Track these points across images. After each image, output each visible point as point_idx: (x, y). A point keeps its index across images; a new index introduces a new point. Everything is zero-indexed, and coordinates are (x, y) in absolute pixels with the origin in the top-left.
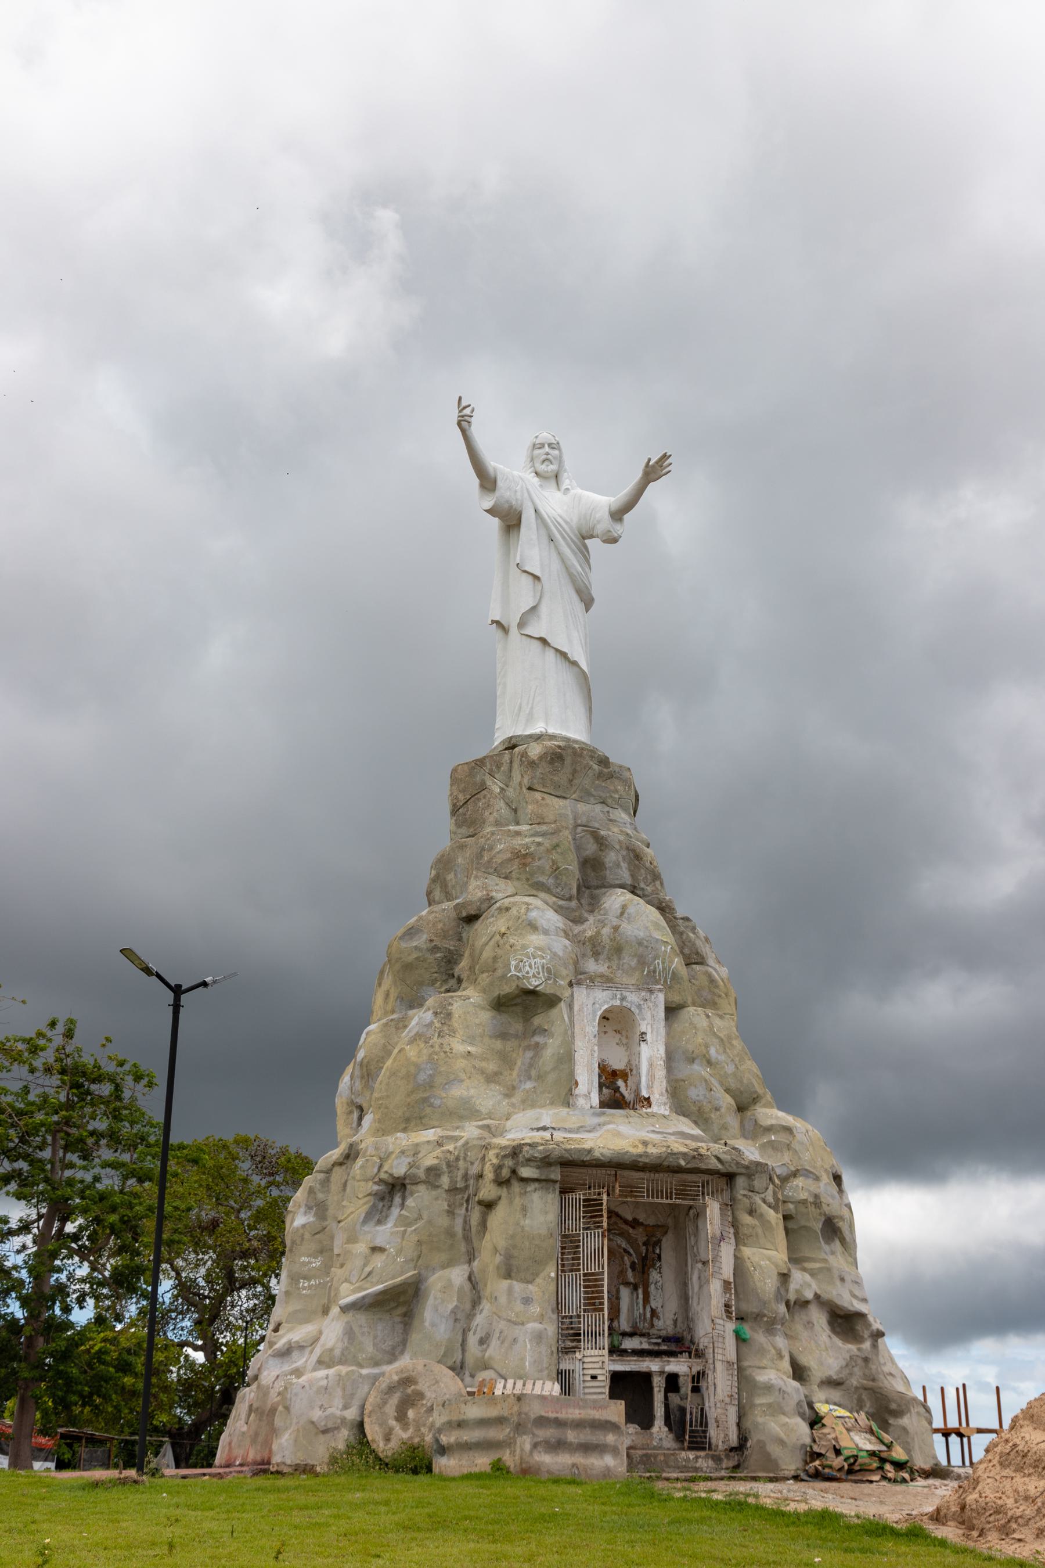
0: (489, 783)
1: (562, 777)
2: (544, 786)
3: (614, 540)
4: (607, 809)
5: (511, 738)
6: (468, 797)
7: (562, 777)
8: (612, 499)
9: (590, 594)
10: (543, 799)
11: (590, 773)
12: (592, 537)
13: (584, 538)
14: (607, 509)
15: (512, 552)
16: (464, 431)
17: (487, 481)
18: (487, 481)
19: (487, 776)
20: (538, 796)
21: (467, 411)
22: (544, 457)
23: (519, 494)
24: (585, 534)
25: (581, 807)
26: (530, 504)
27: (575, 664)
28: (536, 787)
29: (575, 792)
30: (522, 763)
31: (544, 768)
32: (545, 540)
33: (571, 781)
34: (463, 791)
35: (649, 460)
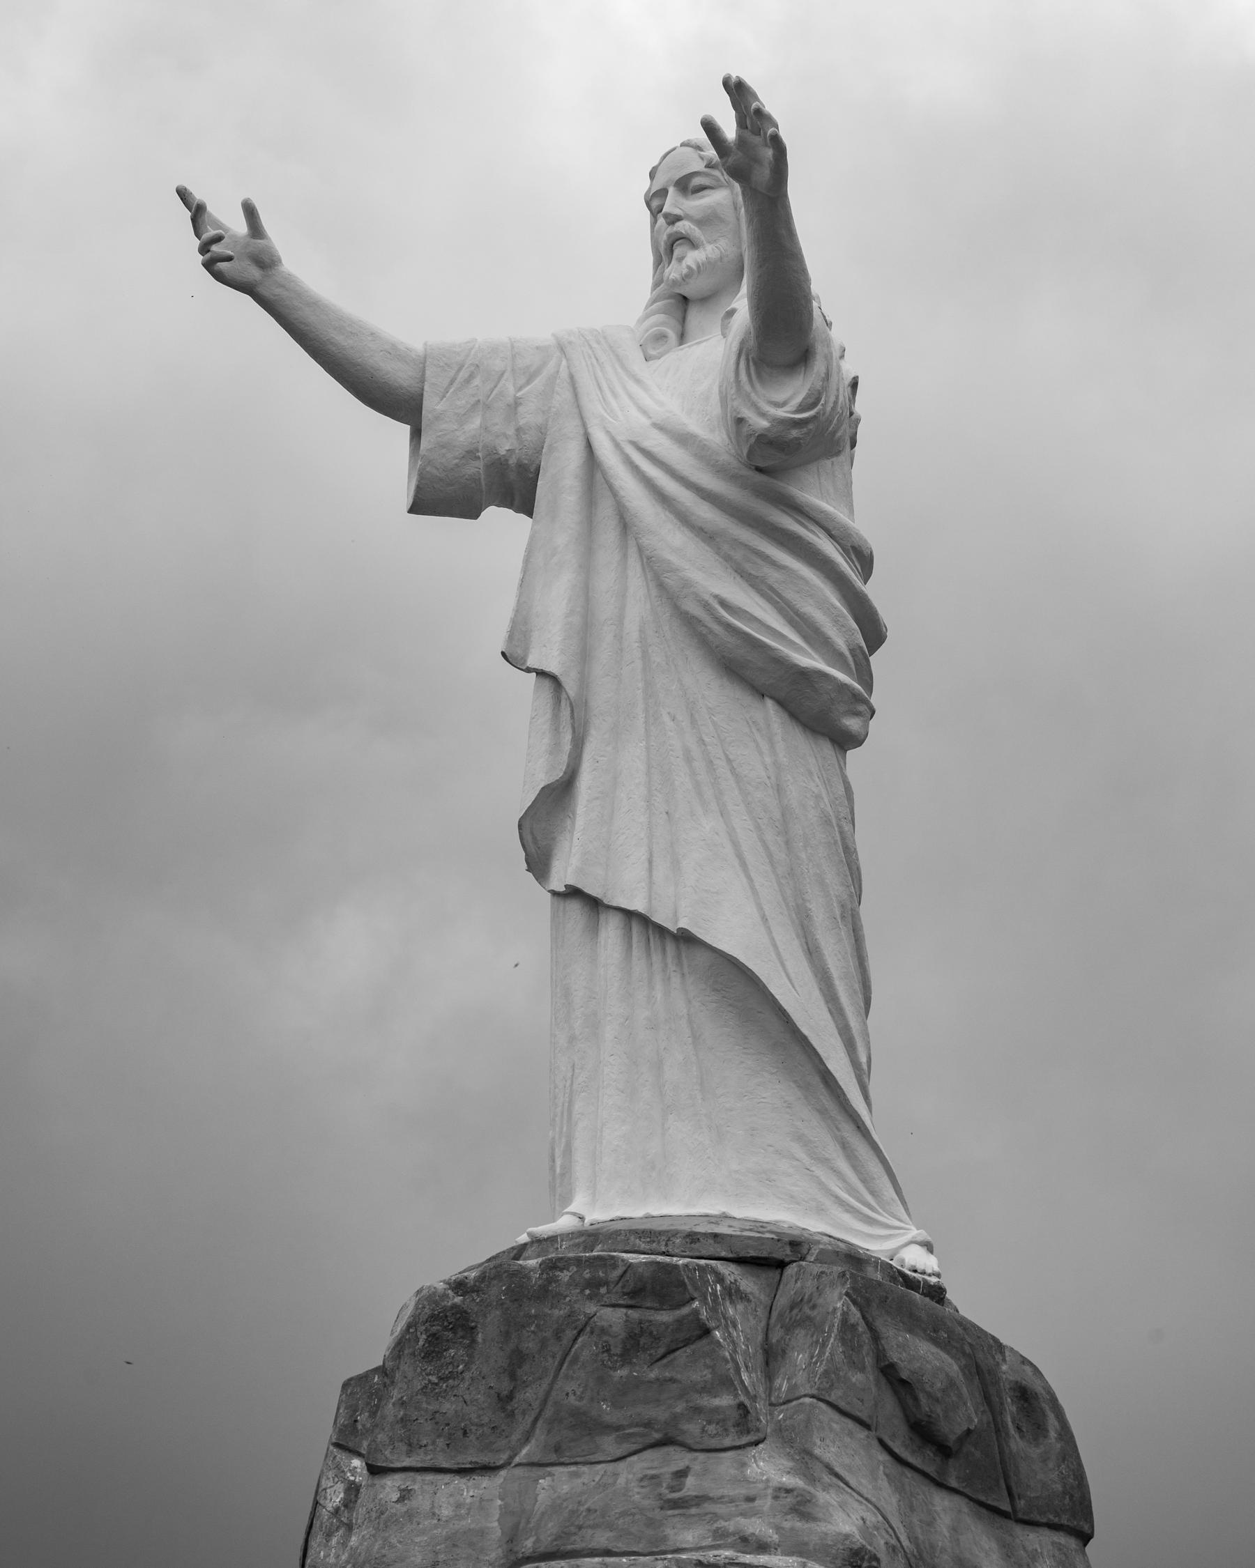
1: (470, 1398)
2: (412, 1447)
7: (470, 1398)
11: (586, 1348)
25: (556, 1486)
29: (527, 1438)
33: (504, 1400)
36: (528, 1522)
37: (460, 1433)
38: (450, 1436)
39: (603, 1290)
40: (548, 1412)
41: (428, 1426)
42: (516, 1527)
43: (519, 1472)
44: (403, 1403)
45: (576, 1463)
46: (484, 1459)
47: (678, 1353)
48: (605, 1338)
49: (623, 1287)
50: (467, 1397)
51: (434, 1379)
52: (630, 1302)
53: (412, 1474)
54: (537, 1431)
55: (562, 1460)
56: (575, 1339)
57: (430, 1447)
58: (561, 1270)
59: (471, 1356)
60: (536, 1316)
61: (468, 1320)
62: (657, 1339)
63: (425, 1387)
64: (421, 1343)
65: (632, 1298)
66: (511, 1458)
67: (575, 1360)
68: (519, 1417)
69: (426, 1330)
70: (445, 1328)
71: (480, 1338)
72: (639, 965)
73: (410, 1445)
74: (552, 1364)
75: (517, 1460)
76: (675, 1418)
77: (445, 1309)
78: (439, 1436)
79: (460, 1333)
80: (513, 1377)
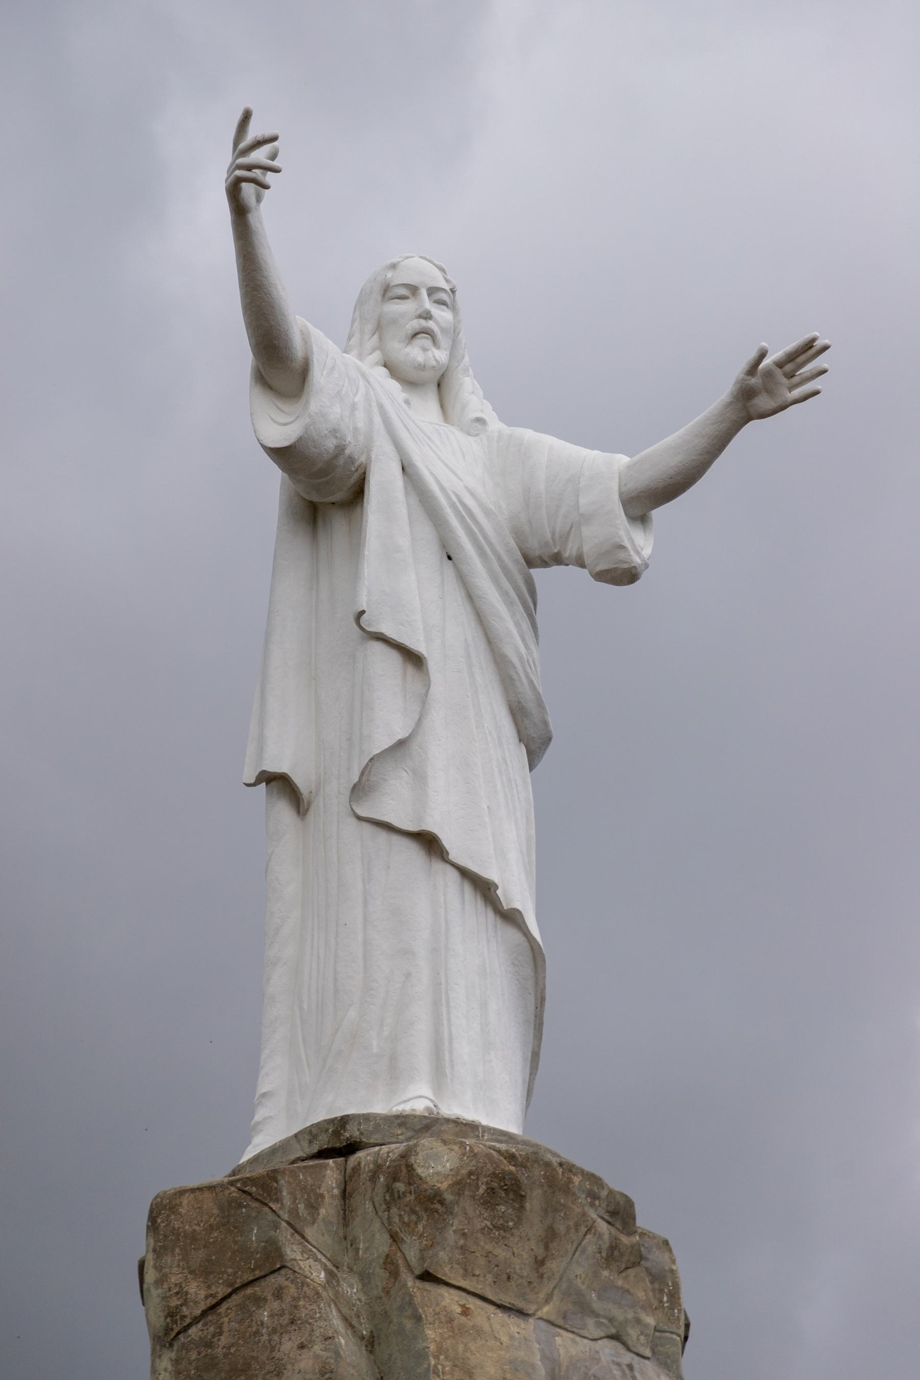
0: (292, 1252)
1: (519, 1253)
2: (467, 1273)
3: (626, 576)
4: (627, 1358)
5: (344, 1121)
6: (221, 1291)
8: (622, 460)
9: (546, 723)
10: (466, 1312)
12: (557, 559)
13: (530, 562)
14: (615, 485)
15: (513, 543)
16: (240, 212)
17: (277, 364)
18: (277, 364)
19: (284, 1235)
20: (450, 1300)
21: (259, 155)
22: (417, 324)
23: (360, 415)
24: (536, 549)
25: (567, 1345)
26: (389, 448)
27: (512, 918)
28: (446, 1272)
29: (547, 1301)
30: (392, 1198)
31: (467, 1216)
32: (431, 555)
34: (205, 1272)
35: (762, 355)
36: (560, 1371)
37: (505, 1277)
38: (497, 1276)
39: (597, 1202)
40: (564, 1285)
41: (482, 1261)
42: (553, 1370)
43: (542, 1324)
44: (464, 1235)
45: (573, 1332)
46: (519, 1304)
47: (629, 1271)
48: (600, 1242)
49: (607, 1205)
50: (515, 1250)
51: (488, 1224)
52: (610, 1220)
53: (464, 1294)
54: (555, 1298)
55: (567, 1326)
56: (585, 1235)
57: (481, 1279)
58: (574, 1175)
59: (519, 1218)
60: (564, 1206)
61: (520, 1188)
62: (622, 1255)
63: (483, 1229)
64: (481, 1191)
65: (611, 1216)
66: (537, 1310)
67: (583, 1252)
68: (545, 1280)
69: (487, 1183)
70: (501, 1187)
71: (528, 1205)
72: (498, 926)
73: (466, 1270)
74: (570, 1248)
75: (539, 1314)
76: (626, 1321)
77: (503, 1172)
78: (490, 1272)
79: (511, 1196)
80: (547, 1248)
